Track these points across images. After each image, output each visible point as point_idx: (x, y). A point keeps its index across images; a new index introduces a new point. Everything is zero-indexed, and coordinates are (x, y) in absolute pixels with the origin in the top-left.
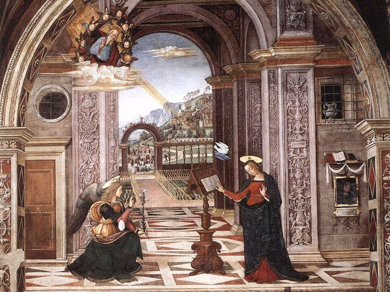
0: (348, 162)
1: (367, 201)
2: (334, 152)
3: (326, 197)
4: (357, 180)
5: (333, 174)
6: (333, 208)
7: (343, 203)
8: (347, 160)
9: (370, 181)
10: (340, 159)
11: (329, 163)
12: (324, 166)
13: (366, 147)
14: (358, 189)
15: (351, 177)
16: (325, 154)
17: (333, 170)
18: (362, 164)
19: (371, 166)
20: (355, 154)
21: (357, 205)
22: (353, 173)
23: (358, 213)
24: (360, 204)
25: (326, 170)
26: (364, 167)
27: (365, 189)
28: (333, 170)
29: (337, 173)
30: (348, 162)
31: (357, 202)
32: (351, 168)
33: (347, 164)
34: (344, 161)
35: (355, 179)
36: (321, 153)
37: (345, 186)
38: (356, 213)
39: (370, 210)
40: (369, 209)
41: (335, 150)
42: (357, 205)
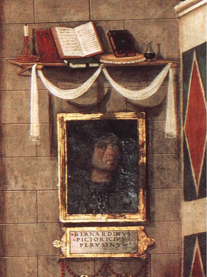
0: (112, 59)
1: (179, 206)
2: (62, 24)
3: (30, 186)
4: (141, 128)
5: (56, 107)
6: (52, 228)
7: (89, 212)
8: (105, 52)
9: (189, 130)
10: (78, 47)
11: (41, 61)
12: (25, 74)
13: (176, 7)
14: (143, 159)
15: (121, 116)
16: (26, 31)
17: (54, 91)
18: (160, 68)
19: (195, 77)
20: (133, 33)
21: (139, 218)
22: (127, 101)
23: (143, 247)
24: (149, 216)
25: (28, 91)
26: (167, 79)
27: (172, 165)
28: (54, 91)
29: (69, 102)
30: (112, 59)
31: (142, 207)
32: (116, 80)
33: (111, 68)
34: (95, 58)
35: (133, 124)
36: (12, 28)
37: (97, 152)
38: (136, 248)
39: (186, 237)
40: (187, 230)
41: (64, 18)
42: (139, 218)
